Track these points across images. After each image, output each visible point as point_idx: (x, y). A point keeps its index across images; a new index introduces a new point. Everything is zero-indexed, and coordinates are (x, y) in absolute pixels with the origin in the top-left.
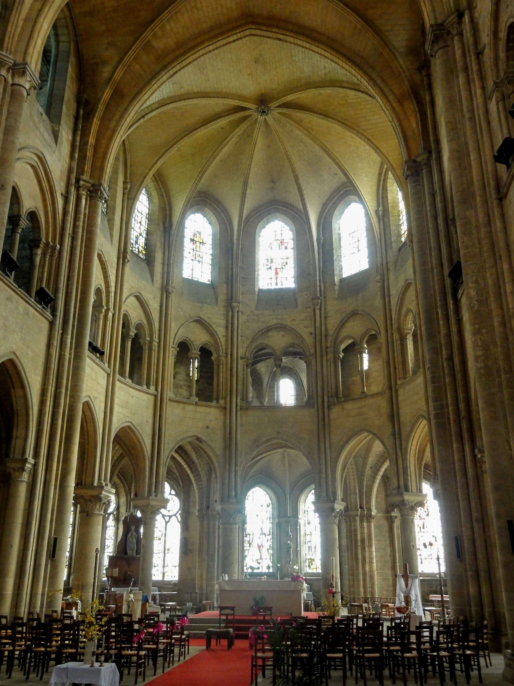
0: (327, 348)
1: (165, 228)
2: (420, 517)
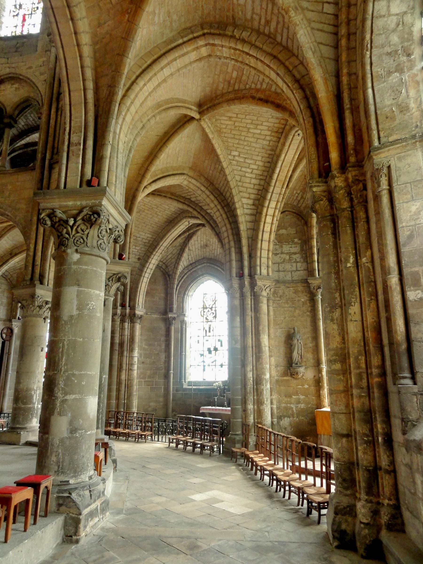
2: (206, 319)
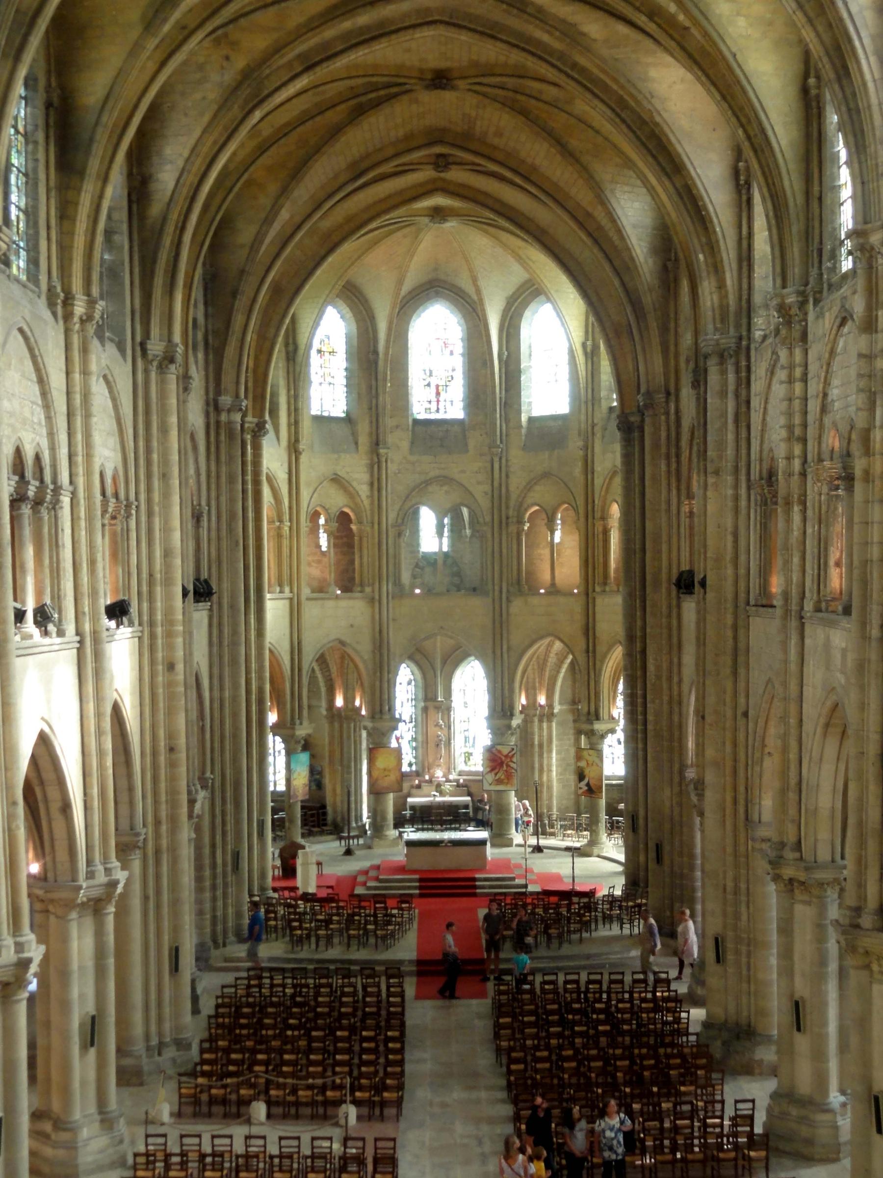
0: (507, 518)
1: (287, 353)
